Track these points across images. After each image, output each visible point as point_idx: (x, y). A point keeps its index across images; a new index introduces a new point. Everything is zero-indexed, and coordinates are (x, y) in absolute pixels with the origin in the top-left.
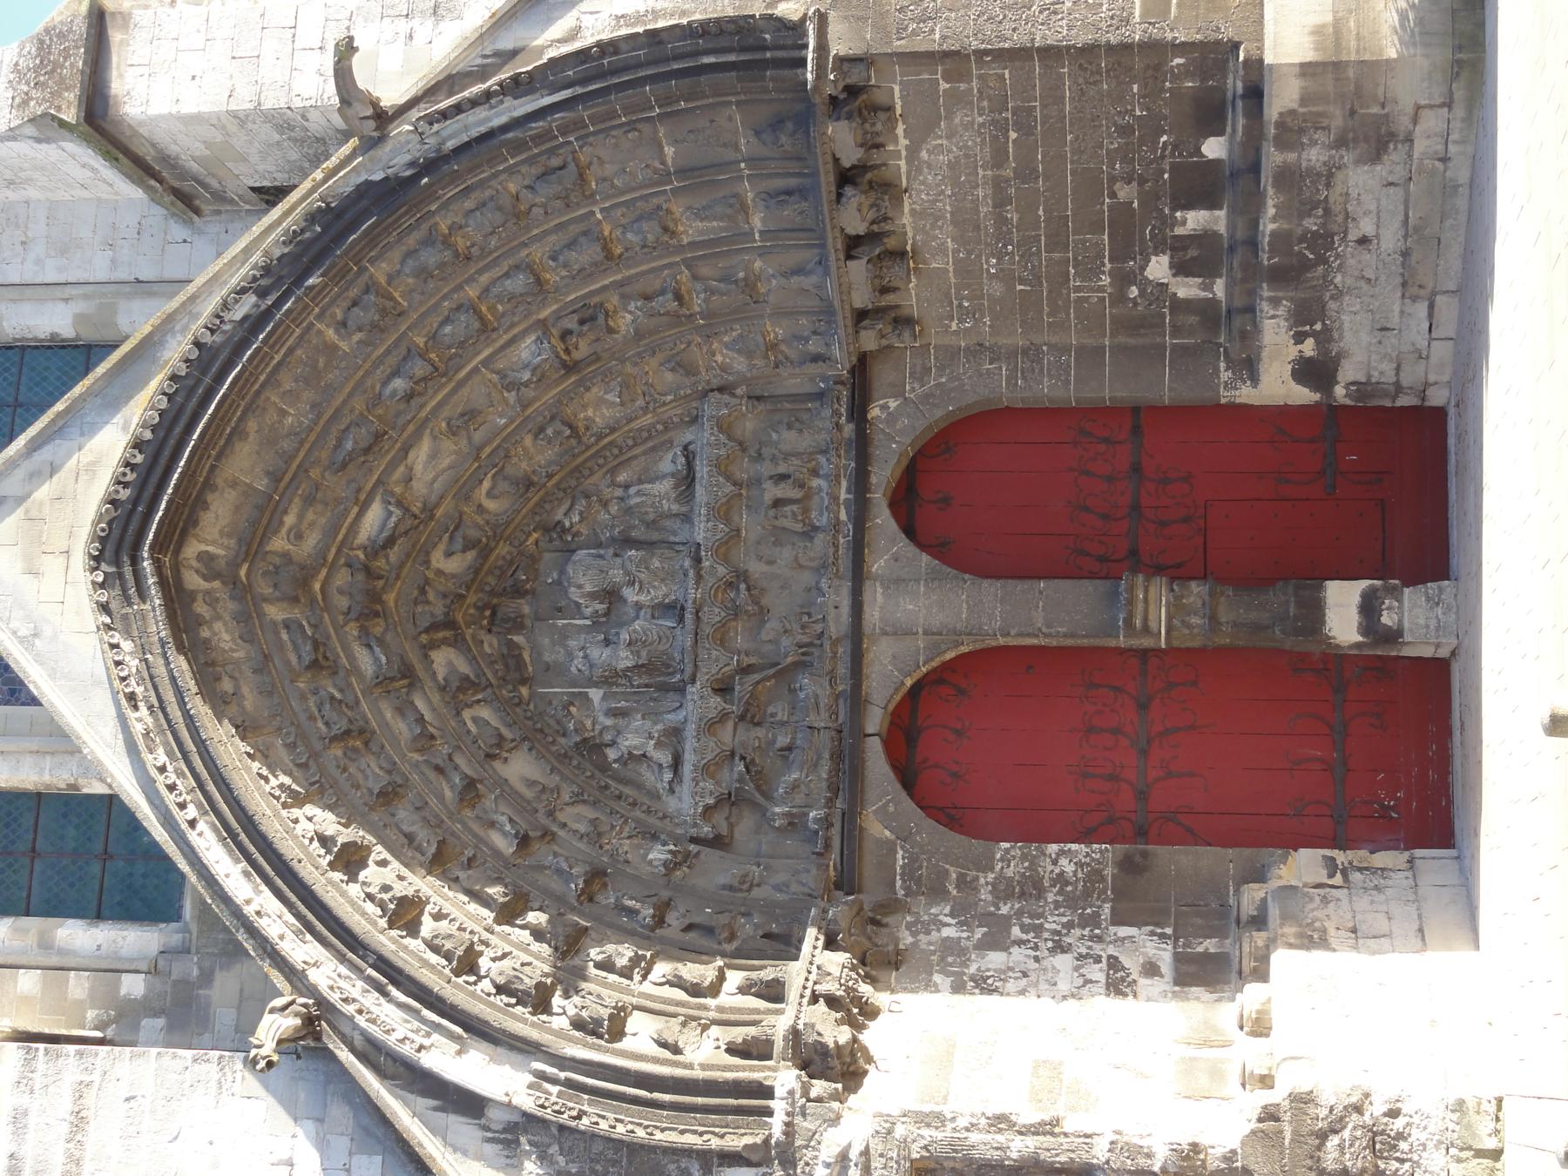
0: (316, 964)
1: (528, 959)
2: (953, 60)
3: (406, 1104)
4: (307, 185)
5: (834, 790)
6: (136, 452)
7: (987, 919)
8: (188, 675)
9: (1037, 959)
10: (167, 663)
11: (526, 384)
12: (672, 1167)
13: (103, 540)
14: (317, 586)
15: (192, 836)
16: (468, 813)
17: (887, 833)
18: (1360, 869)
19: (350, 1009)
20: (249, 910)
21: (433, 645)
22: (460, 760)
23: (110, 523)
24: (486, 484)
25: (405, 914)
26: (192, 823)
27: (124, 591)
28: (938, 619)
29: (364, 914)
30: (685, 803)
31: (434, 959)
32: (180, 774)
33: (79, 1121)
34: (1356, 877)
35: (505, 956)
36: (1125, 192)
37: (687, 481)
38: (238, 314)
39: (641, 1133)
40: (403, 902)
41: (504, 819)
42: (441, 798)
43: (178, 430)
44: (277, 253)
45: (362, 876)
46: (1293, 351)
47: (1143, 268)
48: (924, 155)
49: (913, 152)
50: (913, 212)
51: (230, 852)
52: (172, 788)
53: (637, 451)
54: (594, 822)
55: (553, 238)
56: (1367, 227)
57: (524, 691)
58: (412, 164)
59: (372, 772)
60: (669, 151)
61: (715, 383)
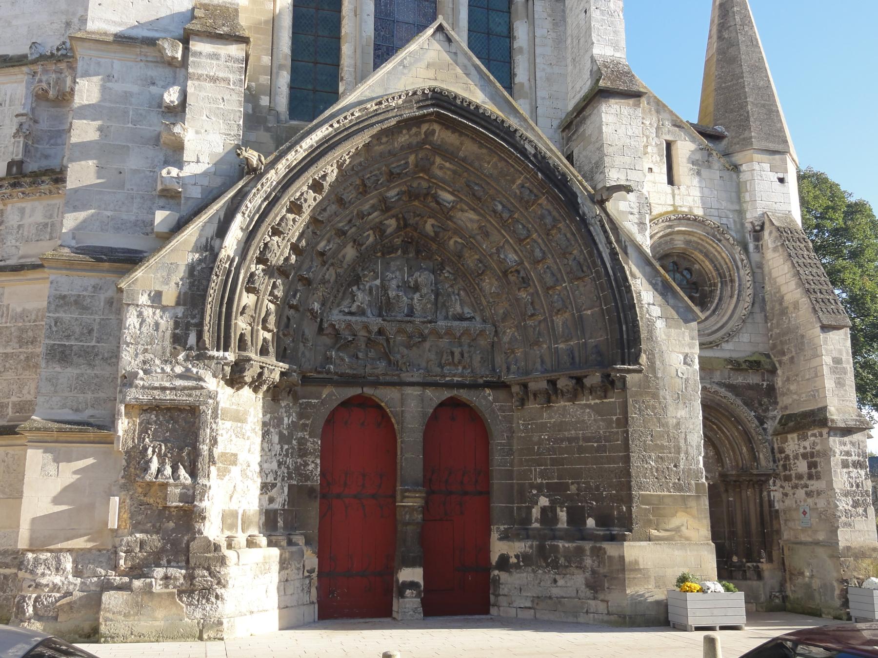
0: (276, 173)
1: (278, 255)
2: (624, 422)
3: (222, 207)
4: (576, 173)
7: (291, 435)
8: (389, 125)
9: (275, 455)
10: (393, 117)
11: (499, 256)
12: (196, 311)
13: (441, 93)
14: (421, 175)
15: (327, 126)
16: (333, 232)
18: (310, 583)
19: (259, 186)
20: (298, 148)
21: (398, 220)
22: (353, 229)
23: (447, 96)
24: (460, 240)
25: (295, 208)
26: (331, 126)
27: (421, 101)
28: (408, 416)
29: (296, 192)
30: (336, 317)
31: (278, 219)
32: (351, 121)
33: (214, 79)
34: (307, 581)
35: (279, 246)
36: (573, 488)
37: (461, 318)
38: (527, 146)
39: (210, 299)
40: (301, 207)
41: (331, 246)
42: (339, 222)
43: (483, 123)
44: (550, 162)
45: (311, 191)
46: (512, 554)
47: (544, 496)
48: (588, 410)
49: (589, 406)
50: (565, 406)
51: (320, 140)
52: (345, 118)
53: (472, 299)
54: (329, 281)
55: (556, 267)
56: (561, 582)
57: (379, 254)
58: (584, 214)
59: (349, 195)
60: (589, 312)
61: (499, 329)
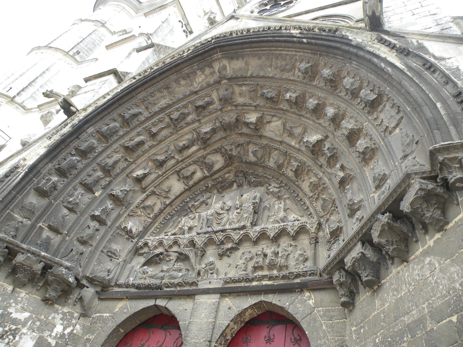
5: (138, 287)
6: (246, 31)
17: (117, 310)
28: (194, 328)
